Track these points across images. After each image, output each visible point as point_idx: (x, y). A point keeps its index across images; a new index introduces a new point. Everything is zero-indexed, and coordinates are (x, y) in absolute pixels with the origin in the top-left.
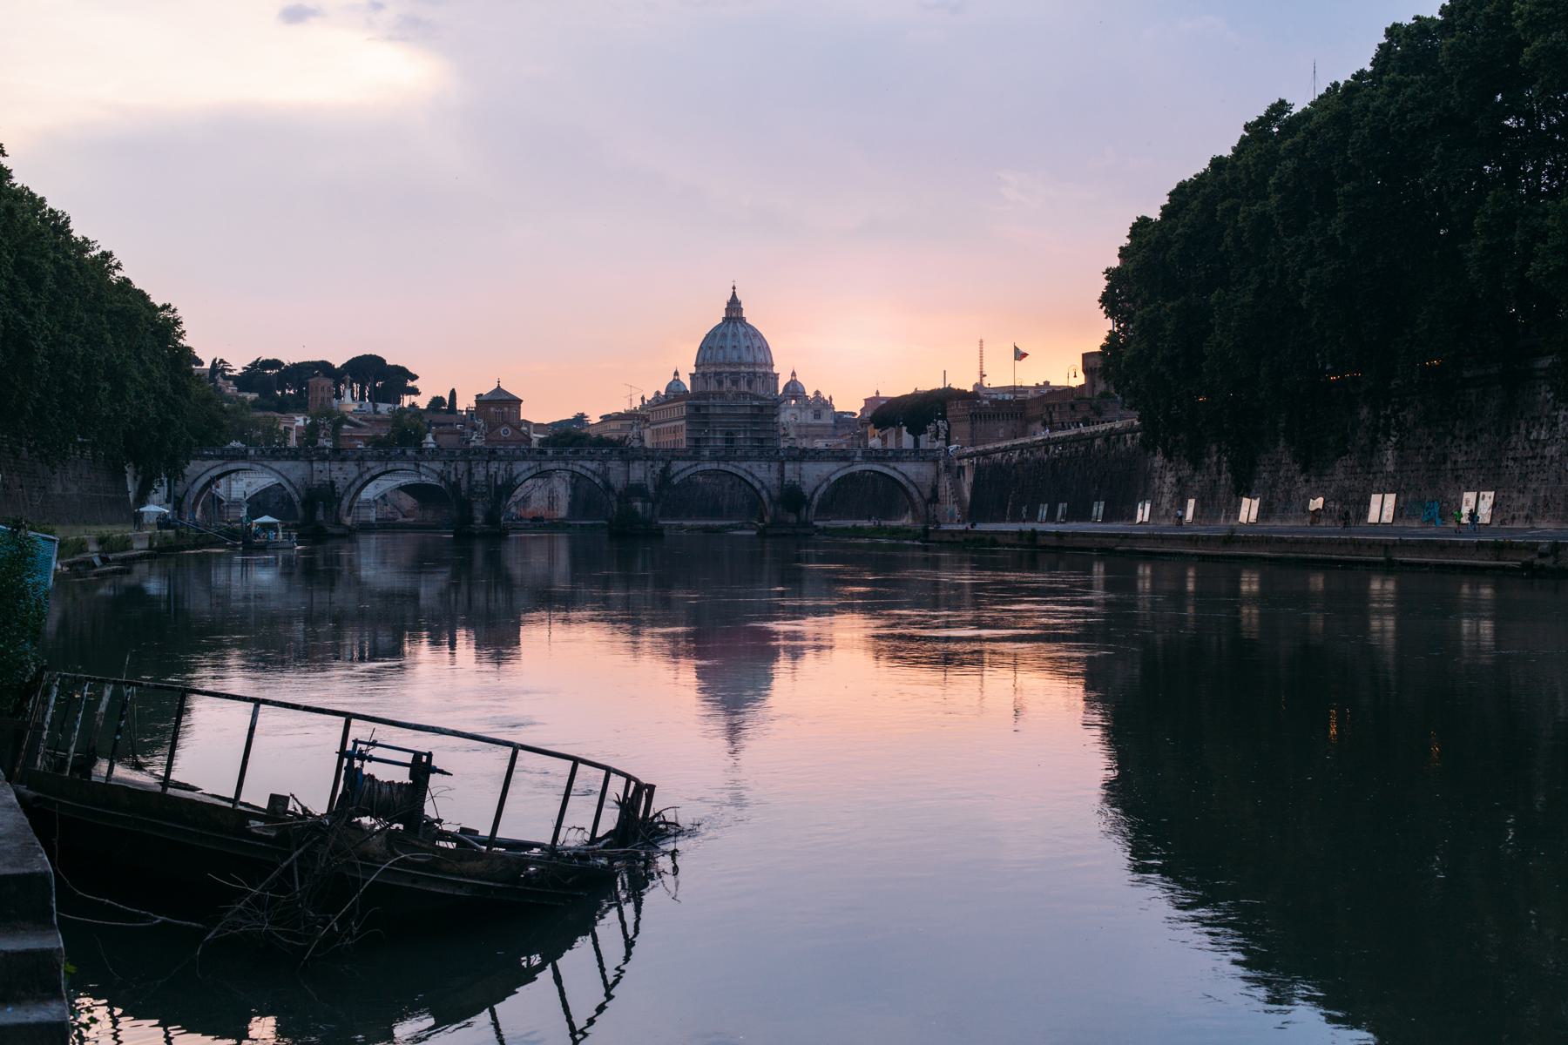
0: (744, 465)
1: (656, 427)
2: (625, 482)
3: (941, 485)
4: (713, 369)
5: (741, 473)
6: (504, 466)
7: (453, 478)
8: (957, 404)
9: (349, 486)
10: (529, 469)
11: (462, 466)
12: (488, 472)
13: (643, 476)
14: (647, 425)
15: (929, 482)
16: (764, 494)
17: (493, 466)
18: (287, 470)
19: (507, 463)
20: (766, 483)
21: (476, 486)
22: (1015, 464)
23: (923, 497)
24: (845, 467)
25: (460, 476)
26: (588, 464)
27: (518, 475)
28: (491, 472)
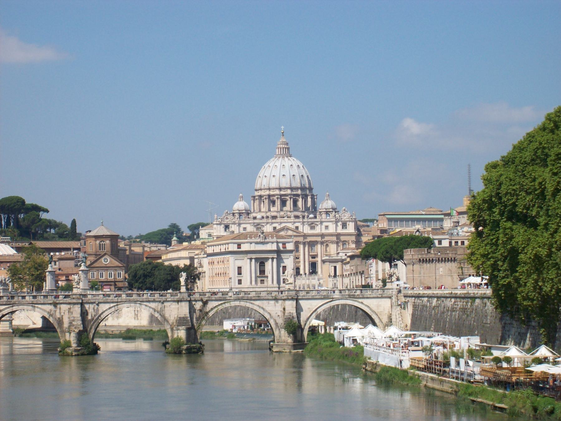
0: (257, 303)
2: (176, 316)
4: (267, 192)
7: (58, 315)
8: (411, 251)
10: (110, 308)
14: (205, 256)
15: (386, 312)
16: (272, 322)
20: (273, 314)
21: (73, 321)
22: (434, 307)
23: (382, 323)
25: (62, 314)
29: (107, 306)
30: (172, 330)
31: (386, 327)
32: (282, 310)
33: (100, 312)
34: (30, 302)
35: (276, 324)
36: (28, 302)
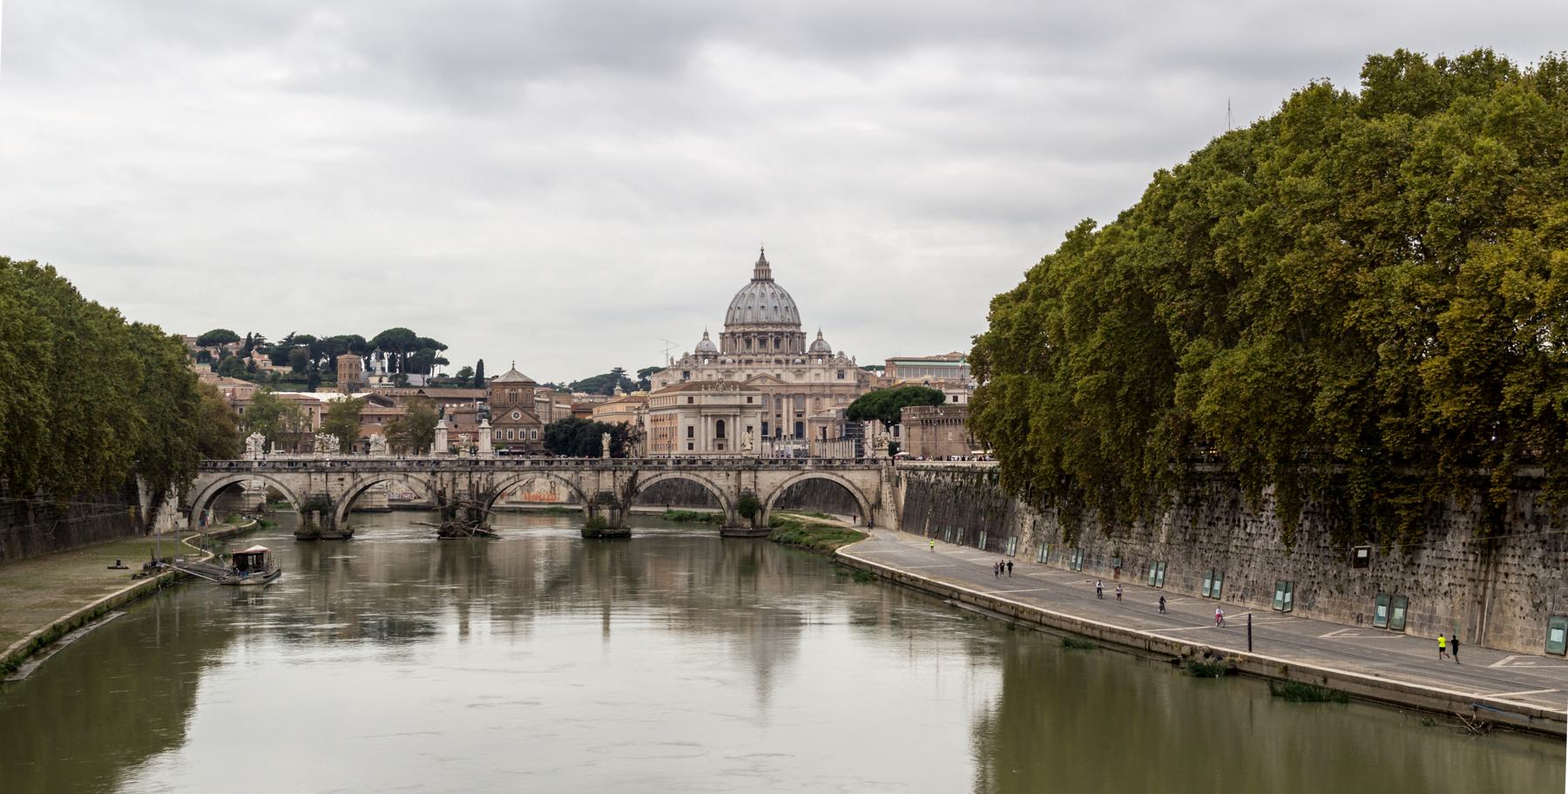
0: (705, 474)
1: (654, 413)
3: (883, 491)
4: (741, 329)
5: (702, 481)
7: (439, 488)
9: (344, 496)
11: (447, 476)
13: (612, 485)
15: (874, 489)
17: (475, 477)
18: (288, 480)
20: (725, 490)
21: (459, 495)
26: (562, 474)
27: (498, 485)
28: (474, 482)
29: (504, 476)
30: (591, 509)
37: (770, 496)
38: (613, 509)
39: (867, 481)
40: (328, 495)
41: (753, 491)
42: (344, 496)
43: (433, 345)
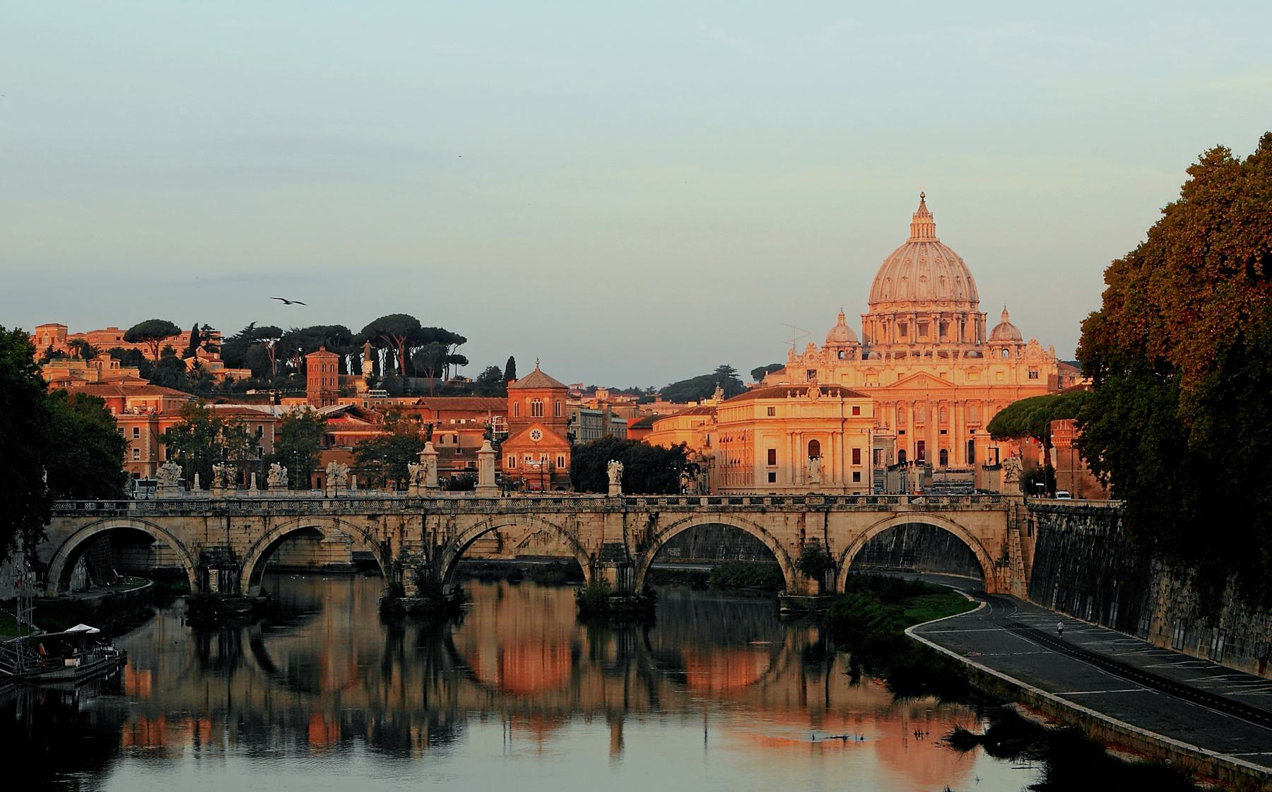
0: (754, 517)
2: (599, 542)
4: (894, 309)
5: (749, 528)
6: (446, 522)
8: (1063, 423)
9: (252, 549)
11: (393, 522)
12: (424, 529)
16: (780, 556)
18: (177, 528)
19: (448, 517)
20: (782, 542)
21: (409, 547)
23: (990, 559)
24: (886, 520)
25: (390, 535)
26: (552, 518)
30: (592, 568)
31: (998, 569)
32: (800, 533)
33: (458, 534)
34: (331, 513)
35: (788, 559)
36: (326, 512)
37: (848, 550)
38: (621, 568)
39: (988, 528)
40: (230, 548)
41: (822, 542)
42: (252, 549)
43: (445, 338)
